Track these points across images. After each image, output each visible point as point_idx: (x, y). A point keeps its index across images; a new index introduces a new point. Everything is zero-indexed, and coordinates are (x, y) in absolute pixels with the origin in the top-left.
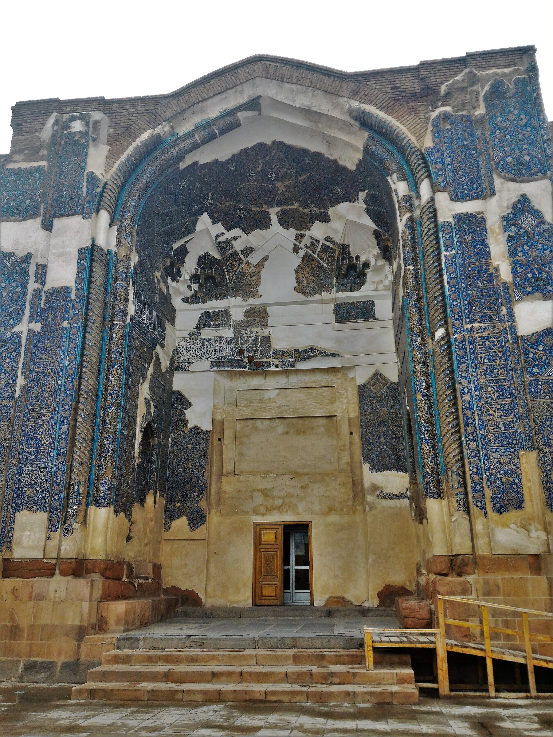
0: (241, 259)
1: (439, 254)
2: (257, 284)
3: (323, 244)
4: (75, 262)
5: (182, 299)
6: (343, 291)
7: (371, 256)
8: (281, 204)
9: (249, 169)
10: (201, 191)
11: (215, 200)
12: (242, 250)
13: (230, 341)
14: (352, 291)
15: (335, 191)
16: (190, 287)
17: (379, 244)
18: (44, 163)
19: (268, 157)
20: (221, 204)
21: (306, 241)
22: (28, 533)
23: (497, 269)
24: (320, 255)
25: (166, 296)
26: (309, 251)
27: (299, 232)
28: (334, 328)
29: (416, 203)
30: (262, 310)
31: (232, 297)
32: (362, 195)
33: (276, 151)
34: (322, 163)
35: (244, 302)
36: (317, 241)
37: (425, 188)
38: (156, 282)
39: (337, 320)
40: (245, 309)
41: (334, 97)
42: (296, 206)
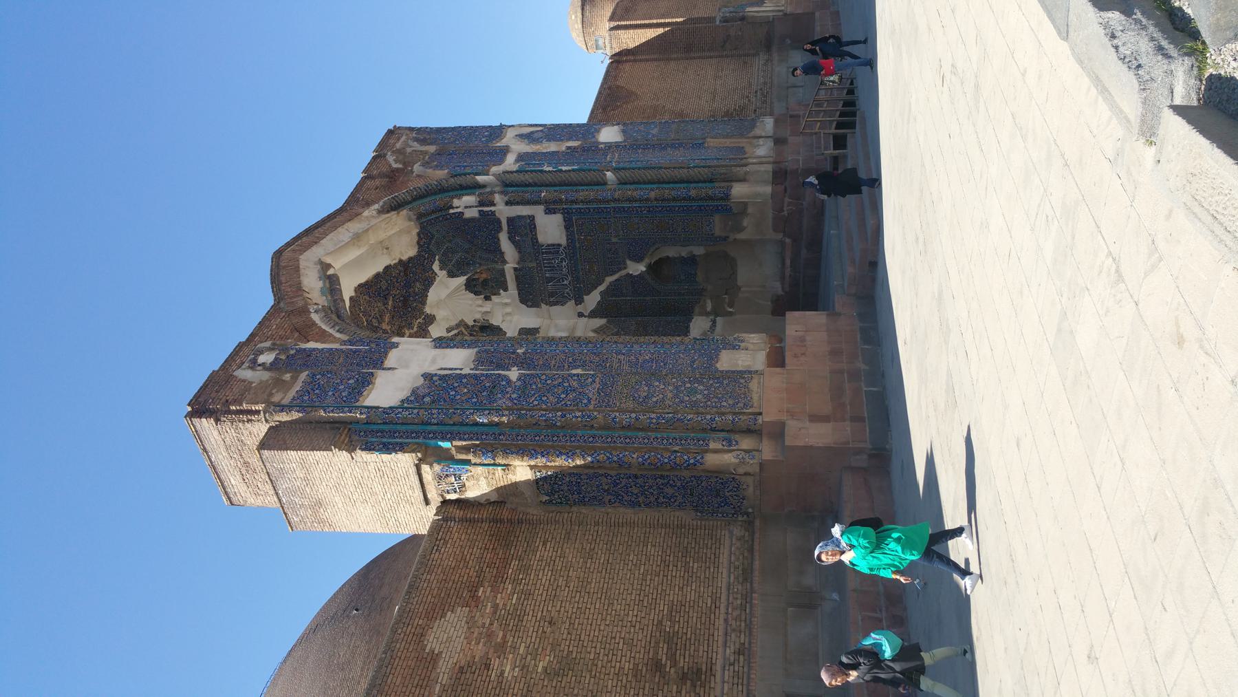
1: (542, 171)
4: (448, 351)
17: (476, 293)
18: (303, 376)
22: (740, 362)
23: (569, 148)
29: (488, 190)
32: (436, 267)
37: (480, 178)
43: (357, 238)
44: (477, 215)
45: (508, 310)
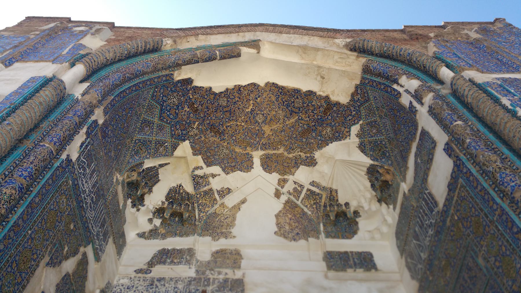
0: (215, 199)
2: (231, 225)
3: (308, 190)
5: (138, 235)
6: (334, 237)
7: (363, 201)
8: (265, 148)
9: (239, 109)
10: (188, 118)
11: (201, 131)
12: (219, 189)
13: (190, 282)
14: (343, 237)
15: (325, 132)
16: (150, 221)
17: (373, 186)
19: (259, 99)
20: (205, 137)
21: (289, 186)
24: (303, 203)
25: (120, 211)
26: (292, 197)
27: (282, 177)
28: (326, 277)
30: (234, 252)
31: (200, 235)
32: (355, 129)
33: (268, 92)
34: (313, 104)
35: (213, 242)
36: (301, 186)
37: (446, 73)
38: (115, 180)
39: (330, 267)
40: (214, 249)
41: (330, 39)
42: (281, 151)
43: (304, 49)
44: (407, 104)
45: (385, 229)
